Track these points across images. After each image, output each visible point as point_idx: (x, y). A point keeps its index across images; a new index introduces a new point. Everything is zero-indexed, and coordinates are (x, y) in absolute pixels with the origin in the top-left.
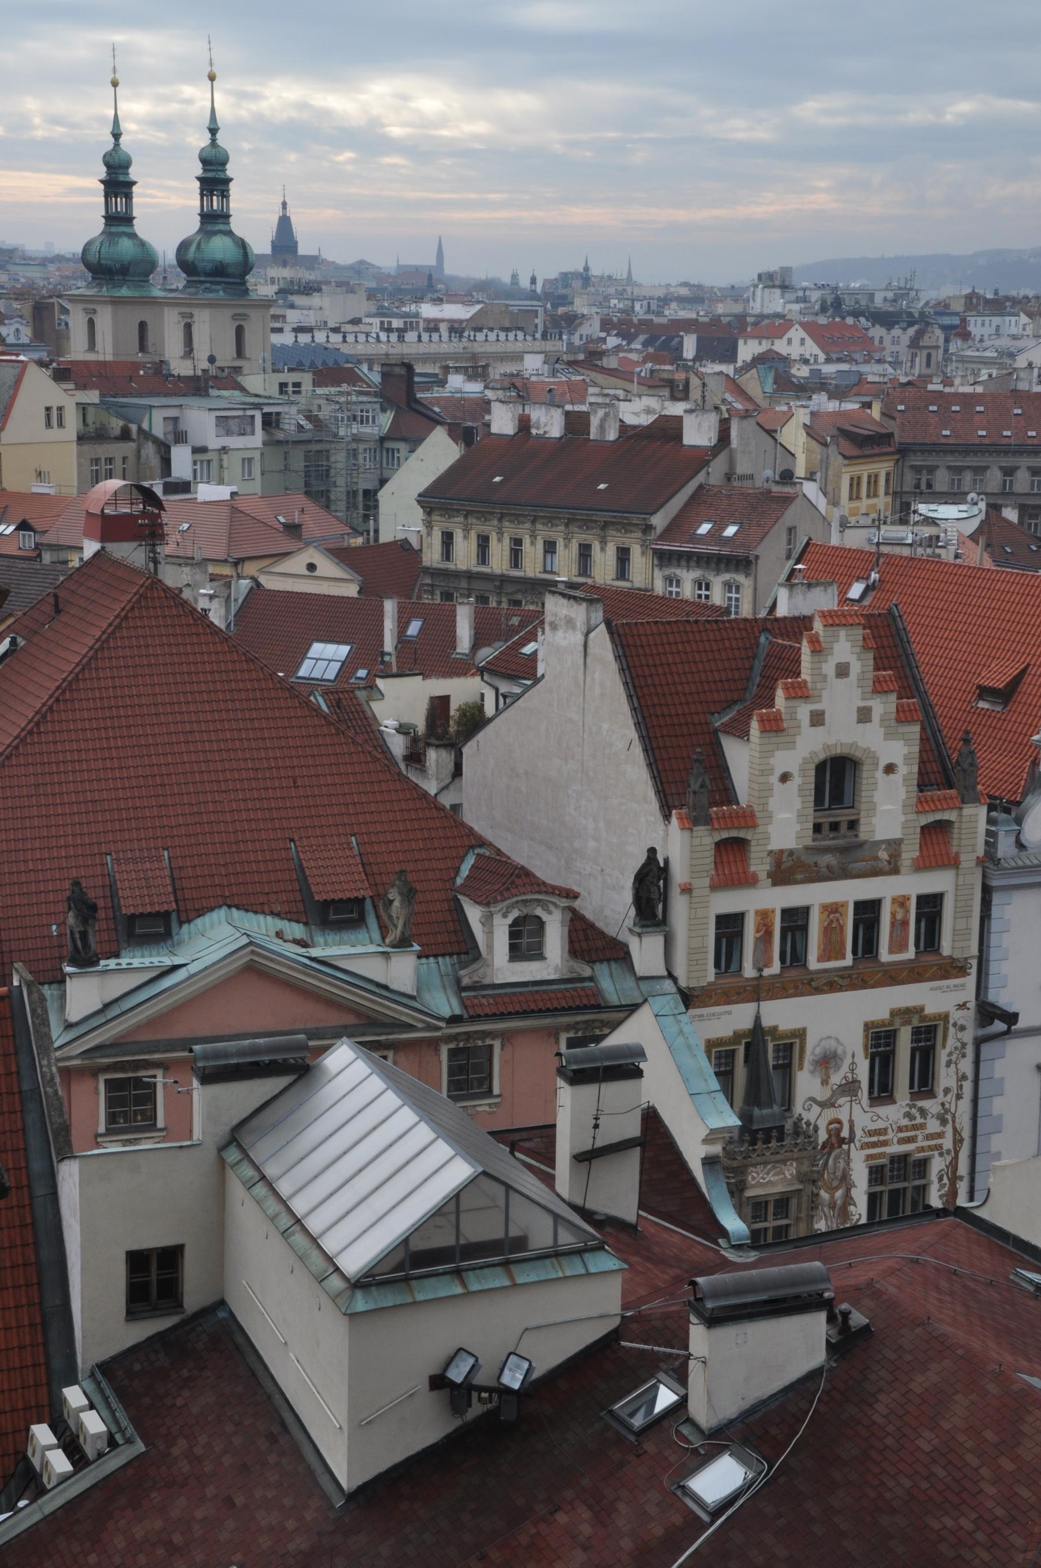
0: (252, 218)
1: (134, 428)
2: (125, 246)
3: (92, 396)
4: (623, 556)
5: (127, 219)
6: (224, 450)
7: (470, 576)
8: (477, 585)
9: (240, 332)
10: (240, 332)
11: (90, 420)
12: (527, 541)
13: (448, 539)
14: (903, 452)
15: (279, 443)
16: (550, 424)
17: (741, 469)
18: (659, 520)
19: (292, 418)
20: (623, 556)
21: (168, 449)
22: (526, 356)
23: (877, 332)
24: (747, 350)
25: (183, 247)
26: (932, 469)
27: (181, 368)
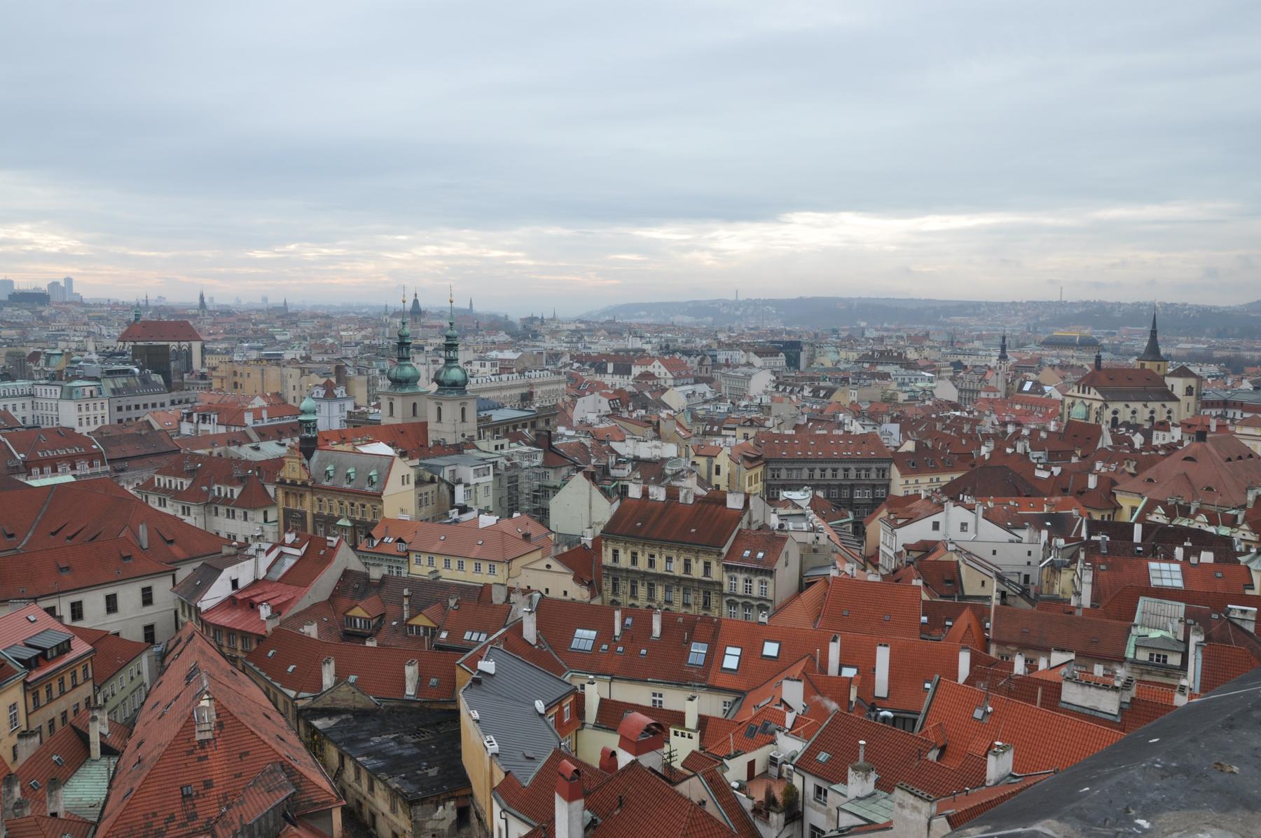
4: (707, 566)
7: (627, 571)
8: (633, 576)
9: (463, 410)
10: (463, 410)
12: (657, 556)
13: (616, 553)
14: (767, 462)
16: (658, 493)
17: (754, 519)
18: (725, 550)
19: (502, 462)
20: (707, 566)
23: (685, 358)
24: (636, 370)
26: (779, 469)
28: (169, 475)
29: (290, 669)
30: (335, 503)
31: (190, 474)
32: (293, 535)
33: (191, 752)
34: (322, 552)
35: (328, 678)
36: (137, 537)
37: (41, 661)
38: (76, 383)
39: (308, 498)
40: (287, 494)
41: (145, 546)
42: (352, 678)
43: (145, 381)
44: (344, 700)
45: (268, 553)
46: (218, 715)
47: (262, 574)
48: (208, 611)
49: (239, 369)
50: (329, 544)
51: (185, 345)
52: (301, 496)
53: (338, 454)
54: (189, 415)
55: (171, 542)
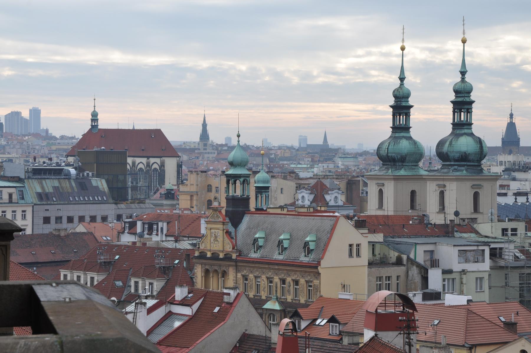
0: (488, 125)
1: (405, 257)
2: (404, 145)
3: (379, 237)
5: (407, 129)
6: (464, 272)
9: (476, 196)
10: (476, 196)
11: (377, 252)
15: (502, 268)
19: (511, 251)
21: (427, 270)
22: (443, 215)
25: (441, 144)
27: (436, 219)
28: (78, 269)
30: (263, 281)
31: (106, 266)
32: (185, 290)
34: (217, 309)
43: (83, 185)
45: (150, 310)
50: (226, 299)
51: (155, 162)
52: (224, 274)
53: (271, 218)
54: (133, 225)
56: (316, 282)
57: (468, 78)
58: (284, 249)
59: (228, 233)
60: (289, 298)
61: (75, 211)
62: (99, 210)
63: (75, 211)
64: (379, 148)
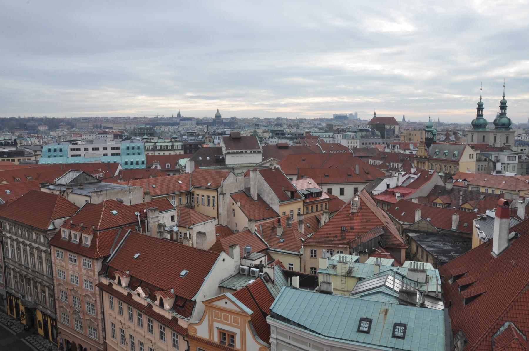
0: (510, 113)
1: (488, 159)
2: (481, 121)
3: (478, 152)
5: (482, 115)
6: (509, 164)
9: (507, 138)
10: (507, 138)
15: (521, 162)
21: (496, 163)
25: (495, 120)
27: (498, 145)
28: (375, 159)
29: (403, 214)
30: (438, 166)
31: (383, 159)
32: (415, 169)
33: (348, 216)
34: (426, 176)
35: (418, 216)
36: (355, 170)
37: (310, 197)
38: (348, 133)
39: (427, 163)
40: (418, 162)
41: (358, 173)
42: (428, 219)
43: (373, 134)
44: (423, 227)
45: (403, 176)
46: (361, 204)
47: (400, 184)
48: (376, 195)
49: (412, 133)
50: (430, 173)
51: (392, 127)
52: (424, 163)
54: (388, 146)
55: (368, 173)
56: (458, 167)
57: (505, 98)
58: (446, 156)
59: (426, 150)
60: (447, 172)
61: (371, 141)
62: (378, 141)
63: (371, 141)
64: (472, 122)
